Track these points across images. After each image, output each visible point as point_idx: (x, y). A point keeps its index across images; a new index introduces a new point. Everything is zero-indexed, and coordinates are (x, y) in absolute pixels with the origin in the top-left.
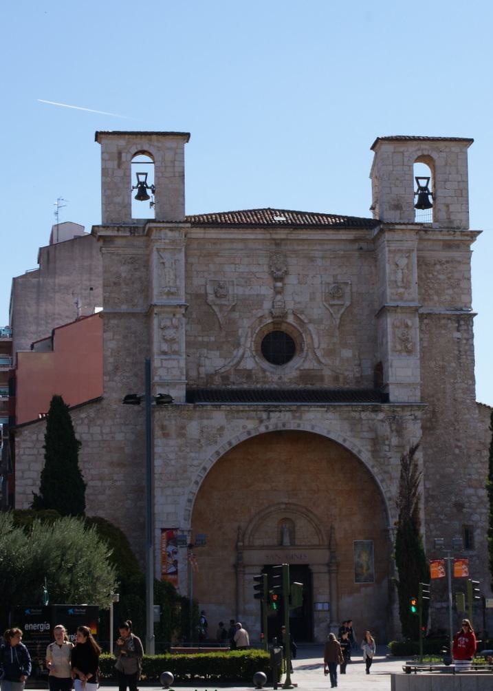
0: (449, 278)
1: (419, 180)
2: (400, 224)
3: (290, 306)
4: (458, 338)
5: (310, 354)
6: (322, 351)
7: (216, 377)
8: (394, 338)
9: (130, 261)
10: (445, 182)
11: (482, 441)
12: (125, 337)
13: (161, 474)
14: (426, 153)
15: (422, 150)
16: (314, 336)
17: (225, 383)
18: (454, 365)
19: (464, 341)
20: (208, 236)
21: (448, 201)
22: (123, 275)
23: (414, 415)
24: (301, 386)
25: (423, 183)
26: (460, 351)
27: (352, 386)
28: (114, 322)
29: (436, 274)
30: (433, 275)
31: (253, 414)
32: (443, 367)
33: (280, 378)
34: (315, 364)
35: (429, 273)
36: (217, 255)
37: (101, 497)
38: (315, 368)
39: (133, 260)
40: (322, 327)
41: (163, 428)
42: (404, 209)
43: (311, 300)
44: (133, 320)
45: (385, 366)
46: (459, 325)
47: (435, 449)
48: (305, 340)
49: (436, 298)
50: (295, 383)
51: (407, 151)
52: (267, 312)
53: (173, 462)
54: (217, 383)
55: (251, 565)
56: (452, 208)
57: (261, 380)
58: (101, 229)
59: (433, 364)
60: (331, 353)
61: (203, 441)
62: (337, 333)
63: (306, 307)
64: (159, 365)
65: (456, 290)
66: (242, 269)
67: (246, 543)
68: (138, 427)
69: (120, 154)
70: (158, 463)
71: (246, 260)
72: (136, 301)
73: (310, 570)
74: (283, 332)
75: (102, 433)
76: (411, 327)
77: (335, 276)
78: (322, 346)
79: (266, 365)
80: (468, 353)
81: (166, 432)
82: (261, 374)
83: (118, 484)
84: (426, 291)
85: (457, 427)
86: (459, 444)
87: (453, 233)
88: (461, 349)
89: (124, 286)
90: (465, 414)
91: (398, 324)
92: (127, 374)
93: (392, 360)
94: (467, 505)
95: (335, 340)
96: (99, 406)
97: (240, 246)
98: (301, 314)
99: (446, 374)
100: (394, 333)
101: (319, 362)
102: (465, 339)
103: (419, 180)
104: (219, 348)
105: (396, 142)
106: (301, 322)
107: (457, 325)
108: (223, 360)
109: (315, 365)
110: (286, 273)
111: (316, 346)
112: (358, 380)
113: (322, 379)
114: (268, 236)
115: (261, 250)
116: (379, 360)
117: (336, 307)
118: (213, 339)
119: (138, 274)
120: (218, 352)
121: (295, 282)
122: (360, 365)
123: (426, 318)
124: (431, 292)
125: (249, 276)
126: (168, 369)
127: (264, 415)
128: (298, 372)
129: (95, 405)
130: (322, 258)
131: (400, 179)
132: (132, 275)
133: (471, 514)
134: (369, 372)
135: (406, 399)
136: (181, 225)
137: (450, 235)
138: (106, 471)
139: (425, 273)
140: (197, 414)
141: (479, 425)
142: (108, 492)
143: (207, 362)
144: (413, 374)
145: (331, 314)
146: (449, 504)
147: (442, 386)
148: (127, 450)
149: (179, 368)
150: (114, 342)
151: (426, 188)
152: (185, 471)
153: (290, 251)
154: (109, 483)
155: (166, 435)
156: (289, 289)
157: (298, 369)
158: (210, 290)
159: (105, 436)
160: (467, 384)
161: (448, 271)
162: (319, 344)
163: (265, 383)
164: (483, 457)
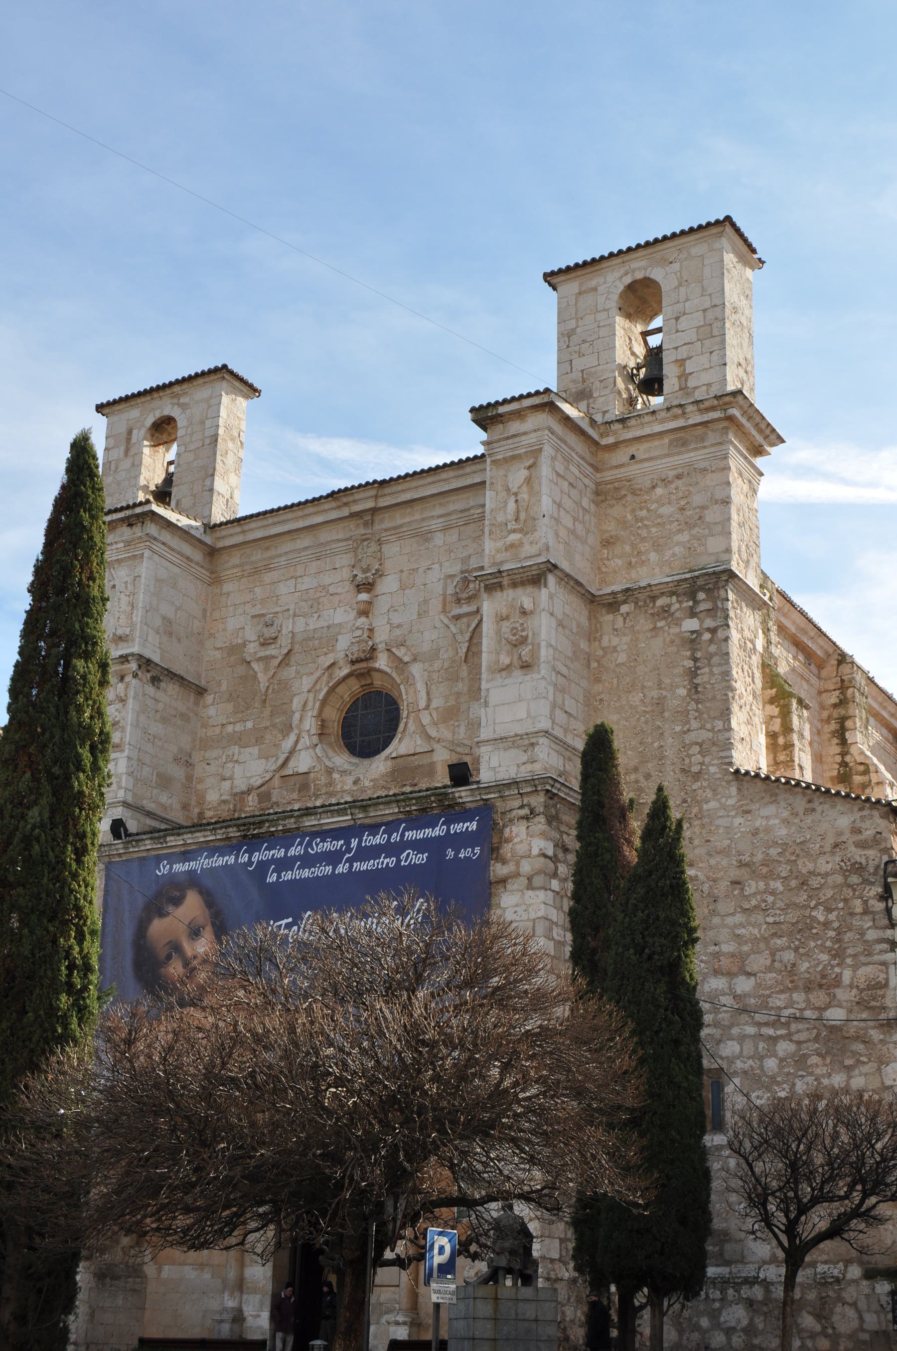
0: (682, 509)
2: (505, 401)
3: (381, 636)
4: (692, 632)
6: (435, 715)
7: (250, 798)
8: (500, 642)
10: (677, 319)
11: (746, 858)
14: (639, 275)
15: (633, 271)
19: (707, 636)
20: (251, 536)
21: (683, 353)
23: (529, 805)
26: (696, 660)
30: (648, 510)
32: (660, 703)
34: (419, 742)
35: (641, 509)
36: (268, 569)
40: (437, 664)
42: (595, 395)
46: (696, 602)
48: (404, 697)
49: (653, 556)
51: (605, 283)
52: (341, 655)
57: (324, 791)
59: (636, 698)
65: (694, 532)
66: (307, 583)
69: (130, 432)
71: (314, 566)
76: (532, 612)
78: (434, 705)
79: (342, 759)
80: (715, 660)
82: (324, 780)
84: (633, 546)
87: (680, 411)
88: (699, 655)
91: (504, 611)
93: (488, 690)
95: (461, 686)
97: (305, 541)
99: (666, 714)
100: (498, 632)
102: (708, 630)
104: (259, 740)
105: (580, 272)
106: (401, 665)
107: (691, 603)
109: (420, 745)
110: (380, 574)
114: (345, 512)
115: (339, 541)
118: (249, 725)
123: (625, 602)
124: (643, 547)
130: (445, 529)
133: (719, 1042)
136: (138, 510)
137: (676, 417)
139: (633, 511)
143: (238, 770)
147: (656, 745)
153: (386, 530)
156: (382, 605)
158: (251, 634)
160: (712, 730)
161: (681, 494)
162: (429, 700)
163: (331, 794)
164: (747, 898)
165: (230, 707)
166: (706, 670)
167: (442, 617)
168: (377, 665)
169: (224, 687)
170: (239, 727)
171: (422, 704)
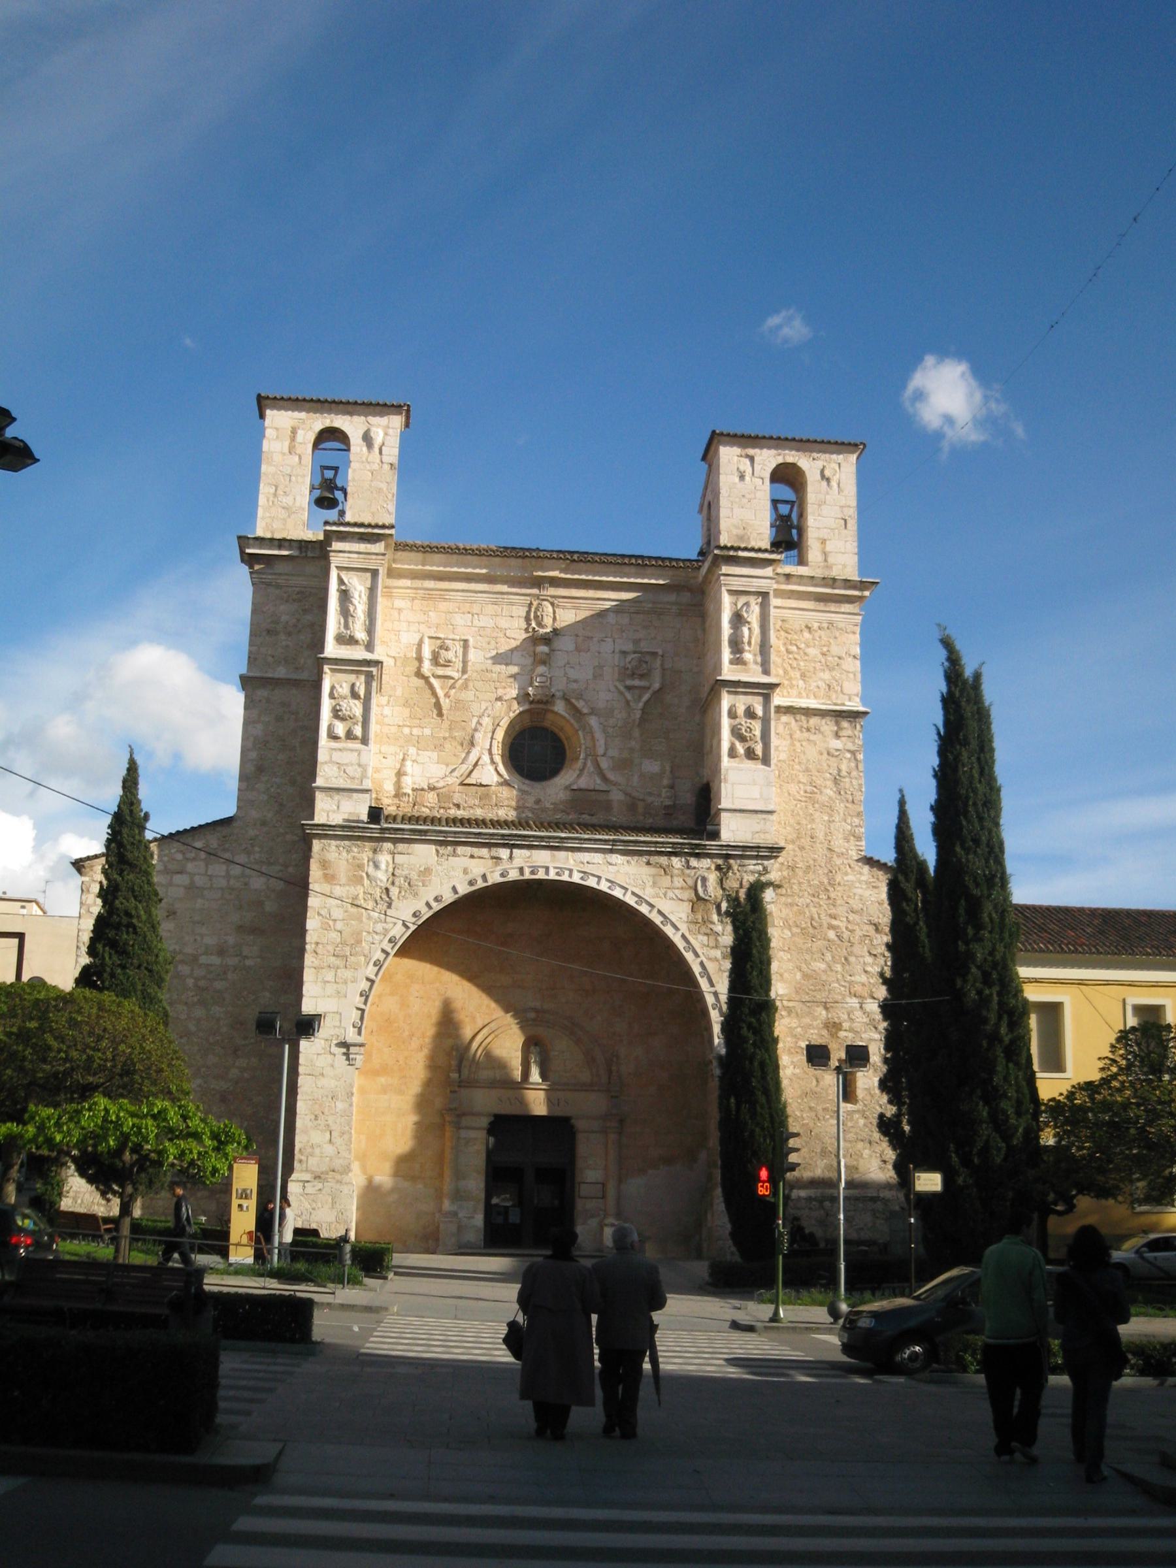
1: (780, 506)
2: (746, 549)
5: (589, 763)
9: (295, 597)
10: (820, 505)
12: (279, 719)
13: (317, 943)
14: (790, 460)
16: (599, 735)
17: (443, 805)
18: (829, 792)
21: (823, 534)
22: (284, 618)
24: (572, 817)
25: (784, 509)
27: (660, 822)
28: (262, 693)
29: (803, 646)
30: (798, 648)
31: (484, 852)
33: (538, 802)
34: (598, 781)
37: (218, 985)
38: (597, 788)
40: (612, 721)
41: (325, 864)
43: (595, 677)
44: (294, 691)
45: (714, 787)
47: (795, 930)
50: (563, 811)
53: (339, 926)
54: (429, 805)
55: (473, 1114)
58: (251, 542)
60: (623, 765)
61: (394, 891)
62: (636, 733)
63: (586, 688)
64: (327, 758)
65: (834, 673)
66: (484, 621)
67: (465, 1072)
68: (291, 869)
69: (294, 431)
70: (312, 924)
71: (490, 609)
72: (302, 661)
73: (572, 1127)
74: (545, 729)
75: (228, 876)
77: (636, 642)
78: (611, 753)
81: (330, 872)
83: (248, 962)
84: (786, 672)
85: (832, 895)
86: (834, 922)
89: (282, 637)
90: (846, 874)
92: (277, 780)
94: (846, 1025)
96: (225, 831)
98: (577, 699)
101: (604, 779)
102: (849, 751)
103: (780, 506)
104: (439, 747)
106: (576, 711)
108: (444, 767)
109: (599, 784)
111: (601, 750)
112: (670, 811)
113: (608, 806)
116: (705, 781)
117: (637, 692)
118: (427, 732)
120: (436, 754)
122: (672, 787)
125: (495, 634)
127: (504, 853)
128: (568, 793)
129: (219, 829)
131: (748, 496)
132: (298, 620)
134: (688, 798)
138: (231, 940)
140: (388, 846)
141: (867, 893)
142: (230, 976)
144: (761, 795)
145: (628, 702)
146: (815, 1023)
148: (269, 907)
149: (359, 765)
150: (260, 726)
151: (789, 517)
152: (359, 942)
154: (236, 960)
155: (330, 878)
156: (560, 659)
157: (567, 788)
159: (232, 882)
162: (606, 749)
165: (407, 712)
166: (847, 780)
167: (617, 684)
168: (556, 709)
169: (399, 692)
170: (415, 731)
171: (601, 751)
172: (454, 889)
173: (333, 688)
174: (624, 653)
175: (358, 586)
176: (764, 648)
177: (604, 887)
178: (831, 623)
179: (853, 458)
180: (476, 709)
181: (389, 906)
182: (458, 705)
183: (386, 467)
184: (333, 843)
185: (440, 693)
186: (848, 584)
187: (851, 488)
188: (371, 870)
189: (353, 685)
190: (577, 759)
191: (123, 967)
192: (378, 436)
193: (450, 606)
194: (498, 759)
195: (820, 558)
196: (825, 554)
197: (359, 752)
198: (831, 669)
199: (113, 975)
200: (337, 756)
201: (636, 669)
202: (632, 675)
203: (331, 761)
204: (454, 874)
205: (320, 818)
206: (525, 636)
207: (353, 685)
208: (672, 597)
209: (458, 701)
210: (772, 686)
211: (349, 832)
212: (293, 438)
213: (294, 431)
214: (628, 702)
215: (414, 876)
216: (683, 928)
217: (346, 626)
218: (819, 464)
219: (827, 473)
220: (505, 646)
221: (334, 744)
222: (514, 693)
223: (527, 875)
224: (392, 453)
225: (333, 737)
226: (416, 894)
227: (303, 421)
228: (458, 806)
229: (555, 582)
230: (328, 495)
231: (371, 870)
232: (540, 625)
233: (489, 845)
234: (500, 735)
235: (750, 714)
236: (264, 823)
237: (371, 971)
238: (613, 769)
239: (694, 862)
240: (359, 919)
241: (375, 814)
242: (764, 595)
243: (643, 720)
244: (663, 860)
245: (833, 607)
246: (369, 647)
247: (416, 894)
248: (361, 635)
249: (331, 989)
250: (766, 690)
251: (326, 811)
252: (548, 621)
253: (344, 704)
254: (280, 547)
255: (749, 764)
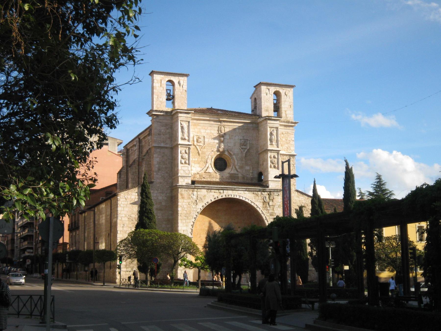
12: (163, 157)
14: (278, 90)
16: (236, 160)
22: (162, 131)
24: (230, 180)
27: (250, 182)
31: (217, 191)
33: (222, 177)
39: (166, 125)
40: (238, 157)
41: (182, 195)
53: (186, 209)
56: (287, 113)
60: (241, 167)
61: (198, 201)
62: (244, 159)
66: (208, 131)
68: (168, 194)
69: (161, 81)
70: (180, 209)
71: (209, 128)
74: (222, 158)
77: (243, 137)
83: (159, 217)
89: (162, 135)
95: (243, 162)
101: (237, 171)
109: (236, 172)
111: (236, 164)
112: (252, 179)
113: (238, 178)
118: (196, 159)
119: (168, 131)
121: (228, 138)
126: (184, 170)
127: (222, 191)
134: (256, 176)
135: (275, 187)
140: (196, 190)
148: (163, 204)
152: (190, 213)
155: (183, 198)
156: (226, 141)
157: (229, 173)
172: (211, 200)
173: (181, 151)
174: (241, 139)
175: (185, 125)
176: (277, 141)
177: (244, 199)
178: (288, 133)
179: (292, 89)
180: (207, 153)
181: (197, 204)
182: (203, 153)
183: (184, 91)
184: (184, 189)
185: (199, 150)
186: (292, 123)
187: (292, 98)
188: (192, 196)
189: (185, 151)
190: (231, 166)
191: (150, 222)
192: (182, 82)
193: (200, 127)
194: (213, 166)
195: (285, 116)
196: (286, 114)
197: (188, 167)
198: (288, 144)
199: (148, 224)
200: (183, 168)
201: (243, 144)
202: (243, 145)
203: (182, 169)
204: (211, 196)
205: (180, 183)
206: (218, 135)
207: (185, 151)
208: (251, 125)
209: (203, 152)
210: (279, 151)
211: (187, 187)
212: (161, 83)
213: (161, 81)
214: (242, 152)
215: (202, 197)
216: (261, 208)
217: (183, 136)
218: (284, 91)
219: (286, 93)
220: (213, 137)
221: (182, 165)
222: (216, 150)
223: (227, 197)
224: (185, 87)
225: (182, 163)
226: (203, 202)
227: (163, 78)
228: (204, 178)
229: (224, 121)
230: (170, 97)
231: (192, 196)
232: (221, 132)
233: (218, 190)
234: (213, 160)
235: (274, 157)
236: (161, 183)
237: (193, 220)
238: (239, 168)
239: (263, 193)
240: (190, 208)
241: (193, 182)
242: (277, 128)
243: (245, 156)
244: (257, 193)
245: (288, 128)
246: (189, 141)
247: (203, 202)
248: (187, 138)
249: (185, 224)
250: (278, 152)
251: (182, 182)
252: (223, 131)
253: (184, 155)
254: (161, 112)
255: (274, 169)
